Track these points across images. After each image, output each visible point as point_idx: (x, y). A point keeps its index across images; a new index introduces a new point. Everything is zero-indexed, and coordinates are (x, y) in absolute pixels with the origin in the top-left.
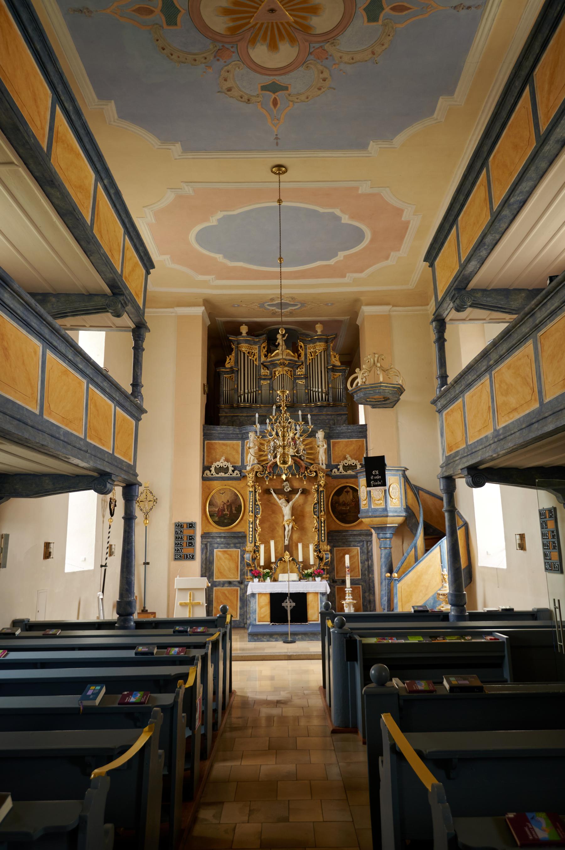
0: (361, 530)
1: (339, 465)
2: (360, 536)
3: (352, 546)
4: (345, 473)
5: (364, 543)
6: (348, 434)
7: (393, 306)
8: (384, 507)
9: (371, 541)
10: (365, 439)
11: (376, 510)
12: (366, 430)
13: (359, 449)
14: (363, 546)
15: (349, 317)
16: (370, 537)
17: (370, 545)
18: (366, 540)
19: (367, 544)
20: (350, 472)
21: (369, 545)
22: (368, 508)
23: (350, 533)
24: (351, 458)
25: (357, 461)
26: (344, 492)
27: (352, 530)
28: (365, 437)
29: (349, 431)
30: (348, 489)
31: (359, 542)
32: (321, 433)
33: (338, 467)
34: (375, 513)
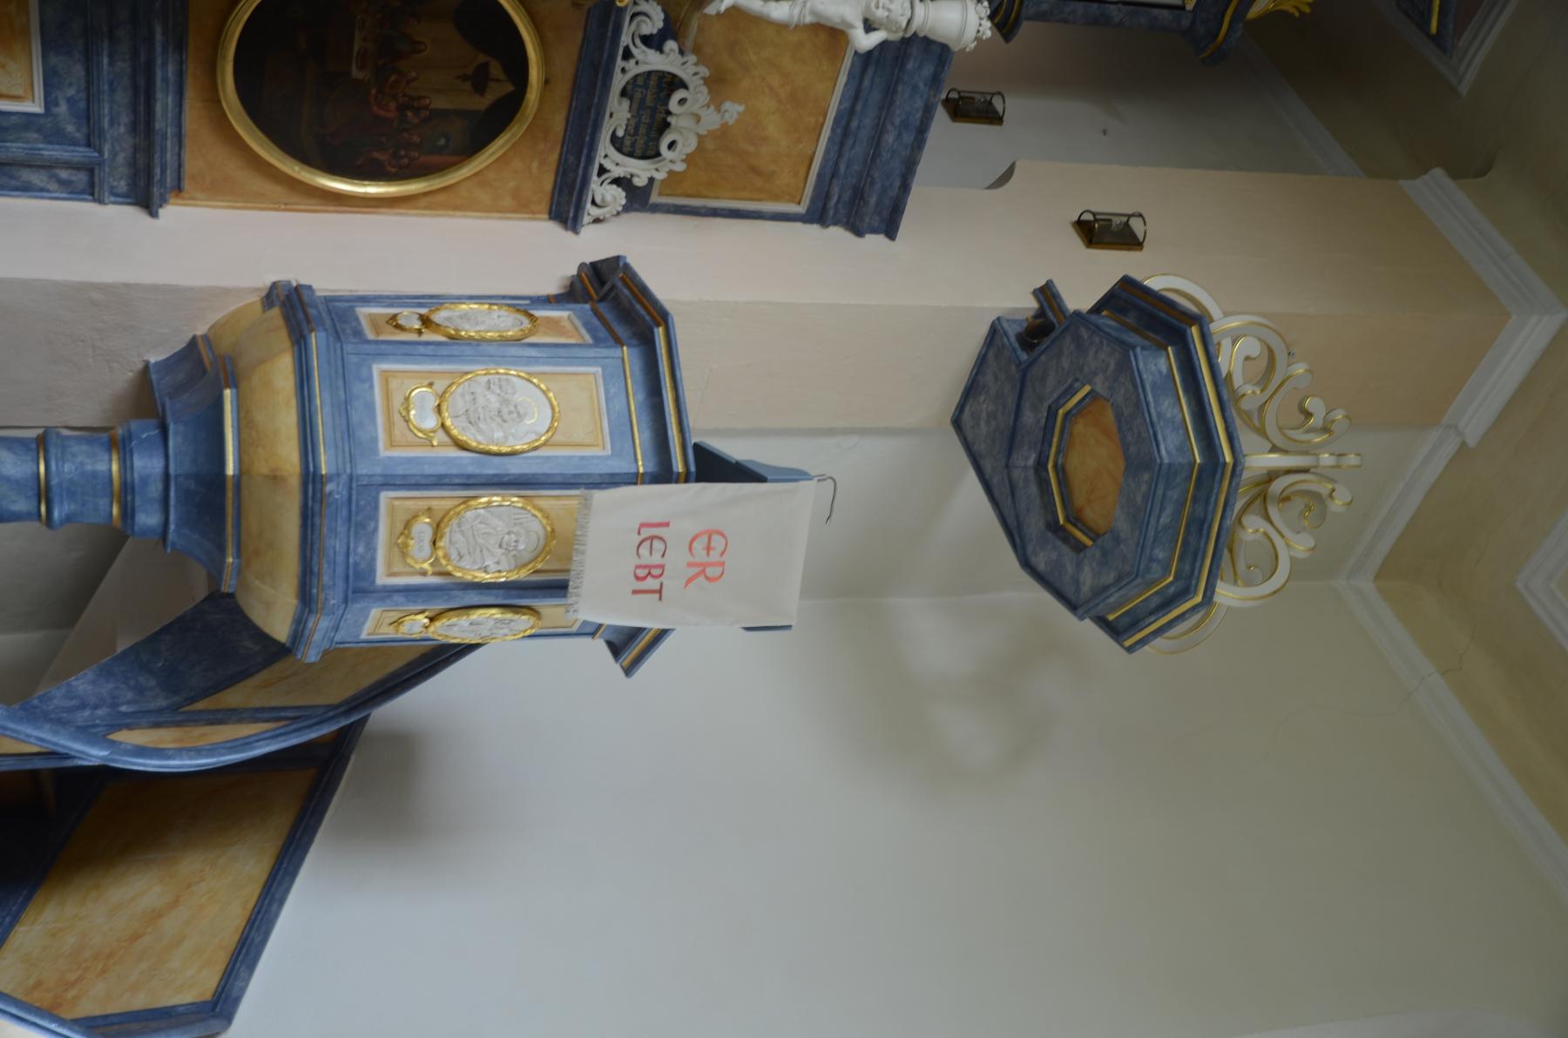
0: (179, 137)
1: (682, 52)
2: (134, 127)
3: (54, 60)
4: (618, 82)
5: (74, 142)
6: (868, 121)
7: (1464, 444)
8: (382, 579)
9: (92, 191)
10: (801, 209)
11: (361, 521)
12: (859, 233)
13: (754, 170)
14: (55, 136)
15: (1464, 89)
16: (122, 186)
17: (64, 184)
18: (101, 164)
19: (69, 165)
20: (618, 115)
21: (64, 174)
22: (384, 451)
23: (165, 71)
24: (713, 135)
25: (680, 167)
26: (482, 58)
27: (181, 74)
28: (818, 215)
29: (889, 138)
30: (499, 89)
31: (88, 117)
32: (970, 33)
33: (671, 45)
34: (345, 513)
